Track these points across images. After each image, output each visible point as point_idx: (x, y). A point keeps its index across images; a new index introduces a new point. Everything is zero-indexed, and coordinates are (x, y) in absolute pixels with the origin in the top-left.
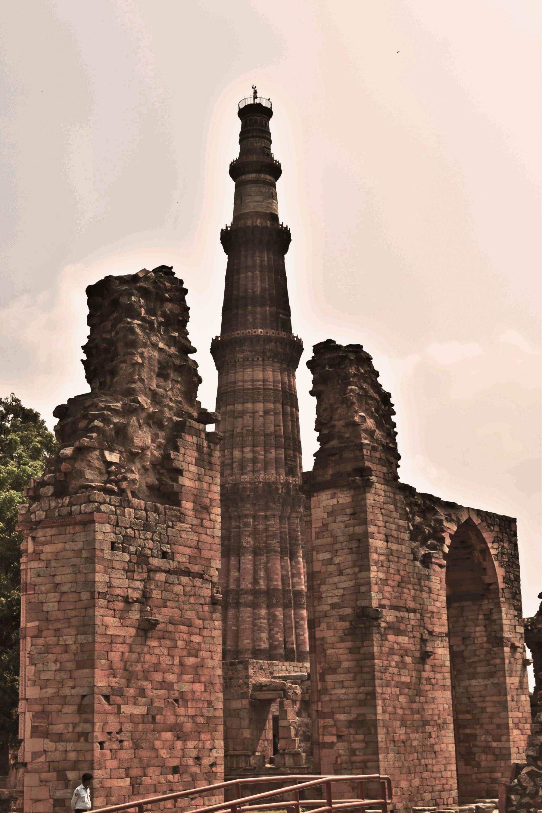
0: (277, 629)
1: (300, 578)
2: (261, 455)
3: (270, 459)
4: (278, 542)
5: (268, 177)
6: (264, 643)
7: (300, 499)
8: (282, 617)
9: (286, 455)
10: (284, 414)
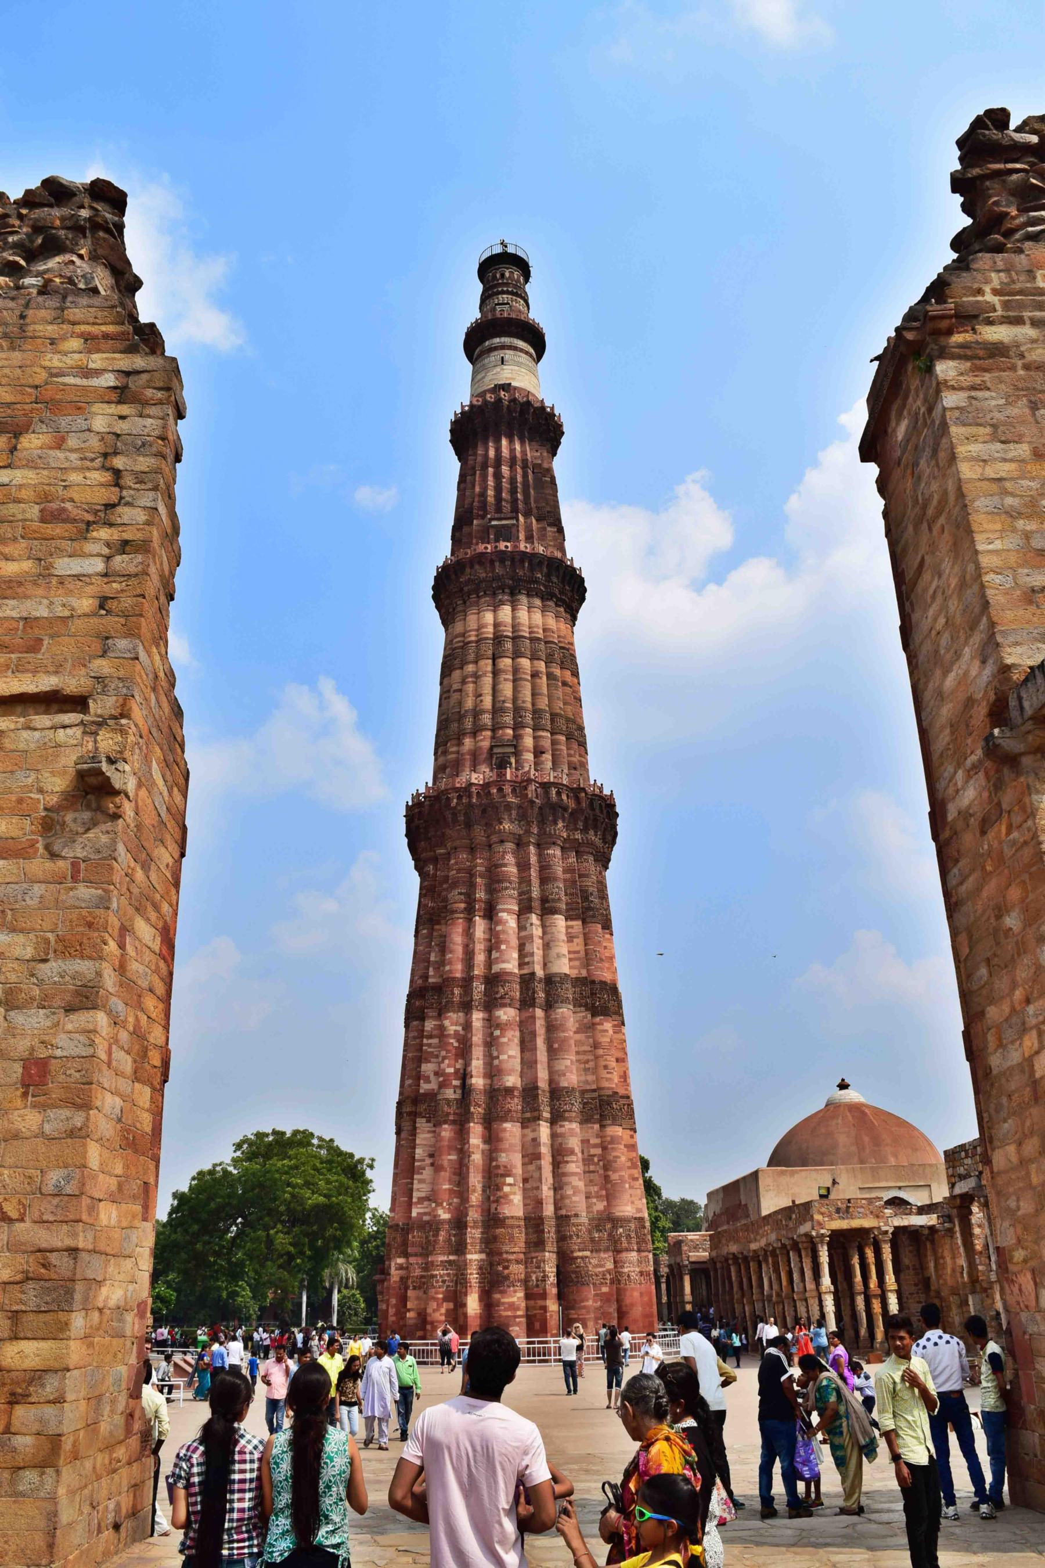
0: (443, 1053)
1: (498, 949)
2: (453, 753)
3: (462, 755)
4: (460, 894)
5: (497, 340)
6: (430, 1082)
7: (497, 808)
8: (459, 1028)
9: (493, 738)
10: (496, 673)
